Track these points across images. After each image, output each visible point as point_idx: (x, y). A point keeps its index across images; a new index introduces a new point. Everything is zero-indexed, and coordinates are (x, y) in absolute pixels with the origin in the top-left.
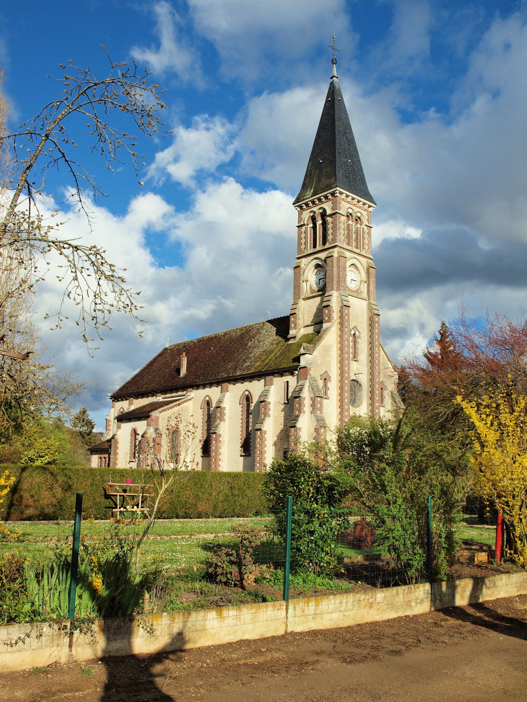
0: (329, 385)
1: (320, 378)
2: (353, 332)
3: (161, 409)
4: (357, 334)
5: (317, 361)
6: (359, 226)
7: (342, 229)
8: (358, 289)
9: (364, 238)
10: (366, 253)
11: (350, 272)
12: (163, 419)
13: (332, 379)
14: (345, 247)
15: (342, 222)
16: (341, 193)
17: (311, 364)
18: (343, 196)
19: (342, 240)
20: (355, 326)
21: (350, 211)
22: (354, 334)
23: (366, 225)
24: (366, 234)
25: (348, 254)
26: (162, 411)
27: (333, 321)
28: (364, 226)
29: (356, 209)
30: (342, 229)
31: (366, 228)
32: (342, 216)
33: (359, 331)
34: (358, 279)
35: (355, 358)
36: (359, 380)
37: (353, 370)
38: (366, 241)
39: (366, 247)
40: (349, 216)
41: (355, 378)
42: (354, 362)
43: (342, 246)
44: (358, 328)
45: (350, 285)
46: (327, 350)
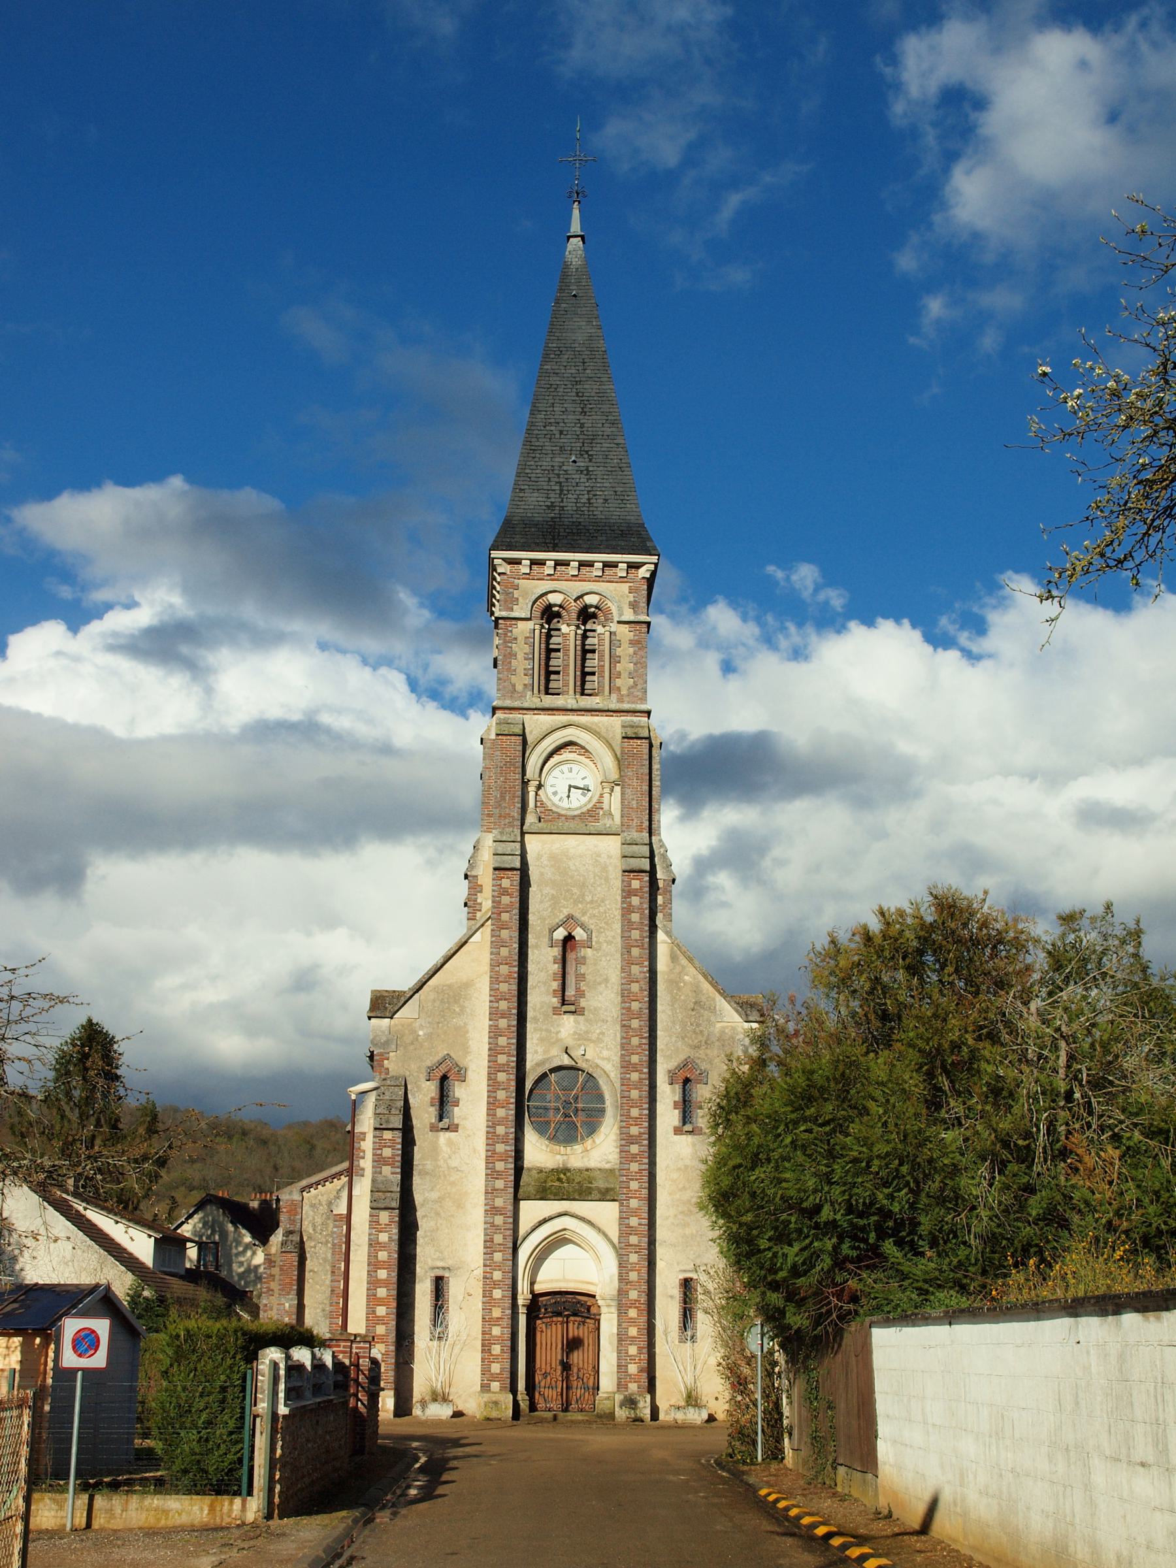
0: (459, 1091)
1: (423, 1076)
2: (560, 934)
3: (304, 1183)
4: (579, 934)
5: (414, 1032)
6: (600, 629)
7: (520, 656)
8: (598, 805)
9: (614, 659)
10: (620, 700)
11: (565, 768)
12: (313, 1206)
13: (471, 1075)
14: (526, 705)
15: (521, 639)
16: (511, 562)
17: (387, 1043)
18: (524, 568)
19: (519, 688)
20: (570, 917)
21: (555, 599)
22: (569, 938)
23: (619, 622)
24: (625, 645)
25: (536, 724)
26: (310, 1186)
27: (479, 914)
28: (614, 627)
29: (577, 588)
30: (520, 656)
31: (624, 632)
32: (520, 624)
33: (583, 927)
34: (592, 782)
35: (567, 1003)
36: (582, 1064)
37: (558, 1040)
38: (625, 666)
39: (624, 683)
40: (550, 614)
41: (566, 1061)
42: (566, 1017)
43: (516, 704)
44: (585, 919)
45: (565, 804)
46: (456, 996)
